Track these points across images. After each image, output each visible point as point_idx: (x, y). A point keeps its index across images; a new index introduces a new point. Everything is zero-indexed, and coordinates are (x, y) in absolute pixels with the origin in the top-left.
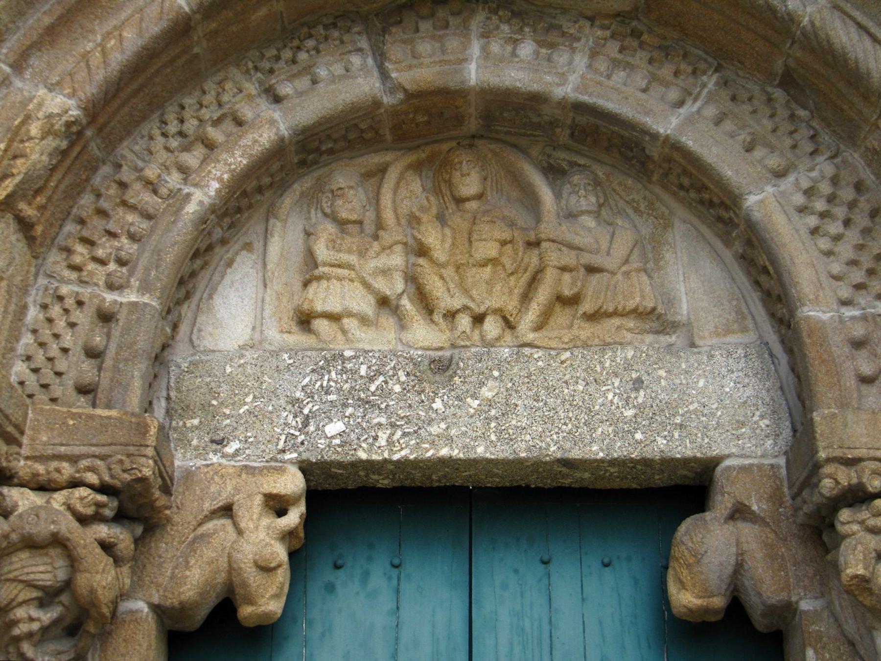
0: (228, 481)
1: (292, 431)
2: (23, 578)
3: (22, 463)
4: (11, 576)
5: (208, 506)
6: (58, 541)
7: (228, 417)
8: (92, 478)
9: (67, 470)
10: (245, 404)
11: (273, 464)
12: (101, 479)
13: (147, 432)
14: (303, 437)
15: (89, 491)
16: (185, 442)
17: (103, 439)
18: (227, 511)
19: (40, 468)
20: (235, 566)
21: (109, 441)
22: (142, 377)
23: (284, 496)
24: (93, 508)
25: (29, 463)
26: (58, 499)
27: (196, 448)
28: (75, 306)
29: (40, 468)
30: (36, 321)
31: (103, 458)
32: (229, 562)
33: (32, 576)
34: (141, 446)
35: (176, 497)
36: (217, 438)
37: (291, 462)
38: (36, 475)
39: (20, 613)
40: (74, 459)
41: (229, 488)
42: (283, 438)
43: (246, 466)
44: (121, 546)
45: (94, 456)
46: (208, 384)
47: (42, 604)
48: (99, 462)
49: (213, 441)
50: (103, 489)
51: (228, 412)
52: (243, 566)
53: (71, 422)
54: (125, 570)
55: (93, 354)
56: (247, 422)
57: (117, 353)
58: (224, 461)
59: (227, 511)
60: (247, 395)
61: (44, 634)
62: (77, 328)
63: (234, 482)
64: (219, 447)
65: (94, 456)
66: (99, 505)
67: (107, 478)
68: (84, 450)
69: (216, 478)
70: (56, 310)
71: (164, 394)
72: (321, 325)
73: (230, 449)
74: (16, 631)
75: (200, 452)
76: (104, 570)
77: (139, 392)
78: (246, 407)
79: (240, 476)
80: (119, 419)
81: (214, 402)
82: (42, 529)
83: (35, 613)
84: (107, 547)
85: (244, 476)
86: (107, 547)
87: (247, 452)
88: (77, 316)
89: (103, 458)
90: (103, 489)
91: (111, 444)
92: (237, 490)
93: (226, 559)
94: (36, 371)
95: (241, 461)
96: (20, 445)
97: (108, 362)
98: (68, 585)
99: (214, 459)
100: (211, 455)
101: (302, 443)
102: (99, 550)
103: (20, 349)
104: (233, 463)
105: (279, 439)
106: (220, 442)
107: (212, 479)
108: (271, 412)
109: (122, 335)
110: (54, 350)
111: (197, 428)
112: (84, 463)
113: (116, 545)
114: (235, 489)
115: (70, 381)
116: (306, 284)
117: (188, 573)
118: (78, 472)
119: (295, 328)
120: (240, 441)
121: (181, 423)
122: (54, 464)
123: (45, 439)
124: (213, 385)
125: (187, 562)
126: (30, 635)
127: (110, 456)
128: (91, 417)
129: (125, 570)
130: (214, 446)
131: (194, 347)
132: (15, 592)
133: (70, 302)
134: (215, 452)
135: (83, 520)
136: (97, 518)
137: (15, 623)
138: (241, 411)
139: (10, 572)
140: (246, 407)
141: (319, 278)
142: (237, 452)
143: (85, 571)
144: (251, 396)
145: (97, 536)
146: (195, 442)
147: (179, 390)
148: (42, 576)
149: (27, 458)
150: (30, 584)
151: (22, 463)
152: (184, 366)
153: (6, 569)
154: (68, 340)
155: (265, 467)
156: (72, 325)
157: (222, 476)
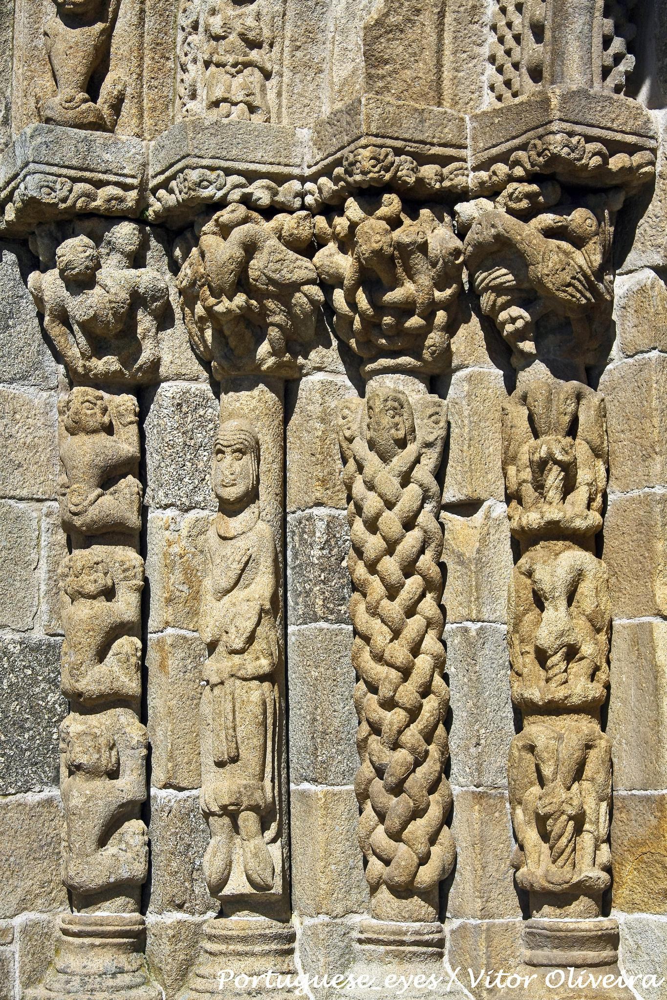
8: (519, 171)
12: (525, 169)
25: (476, 173)
30: (494, 15)
31: (524, 147)
33: (498, 281)
34: (546, 124)
40: (503, 158)
48: (520, 153)
50: (530, 178)
77: (576, 57)
84: (550, 233)
86: (550, 233)
89: (524, 147)
91: (525, 132)
96: (465, 161)
135: (525, 216)
149: (475, 169)
150: (499, 290)
151: (472, 174)
153: (479, 280)
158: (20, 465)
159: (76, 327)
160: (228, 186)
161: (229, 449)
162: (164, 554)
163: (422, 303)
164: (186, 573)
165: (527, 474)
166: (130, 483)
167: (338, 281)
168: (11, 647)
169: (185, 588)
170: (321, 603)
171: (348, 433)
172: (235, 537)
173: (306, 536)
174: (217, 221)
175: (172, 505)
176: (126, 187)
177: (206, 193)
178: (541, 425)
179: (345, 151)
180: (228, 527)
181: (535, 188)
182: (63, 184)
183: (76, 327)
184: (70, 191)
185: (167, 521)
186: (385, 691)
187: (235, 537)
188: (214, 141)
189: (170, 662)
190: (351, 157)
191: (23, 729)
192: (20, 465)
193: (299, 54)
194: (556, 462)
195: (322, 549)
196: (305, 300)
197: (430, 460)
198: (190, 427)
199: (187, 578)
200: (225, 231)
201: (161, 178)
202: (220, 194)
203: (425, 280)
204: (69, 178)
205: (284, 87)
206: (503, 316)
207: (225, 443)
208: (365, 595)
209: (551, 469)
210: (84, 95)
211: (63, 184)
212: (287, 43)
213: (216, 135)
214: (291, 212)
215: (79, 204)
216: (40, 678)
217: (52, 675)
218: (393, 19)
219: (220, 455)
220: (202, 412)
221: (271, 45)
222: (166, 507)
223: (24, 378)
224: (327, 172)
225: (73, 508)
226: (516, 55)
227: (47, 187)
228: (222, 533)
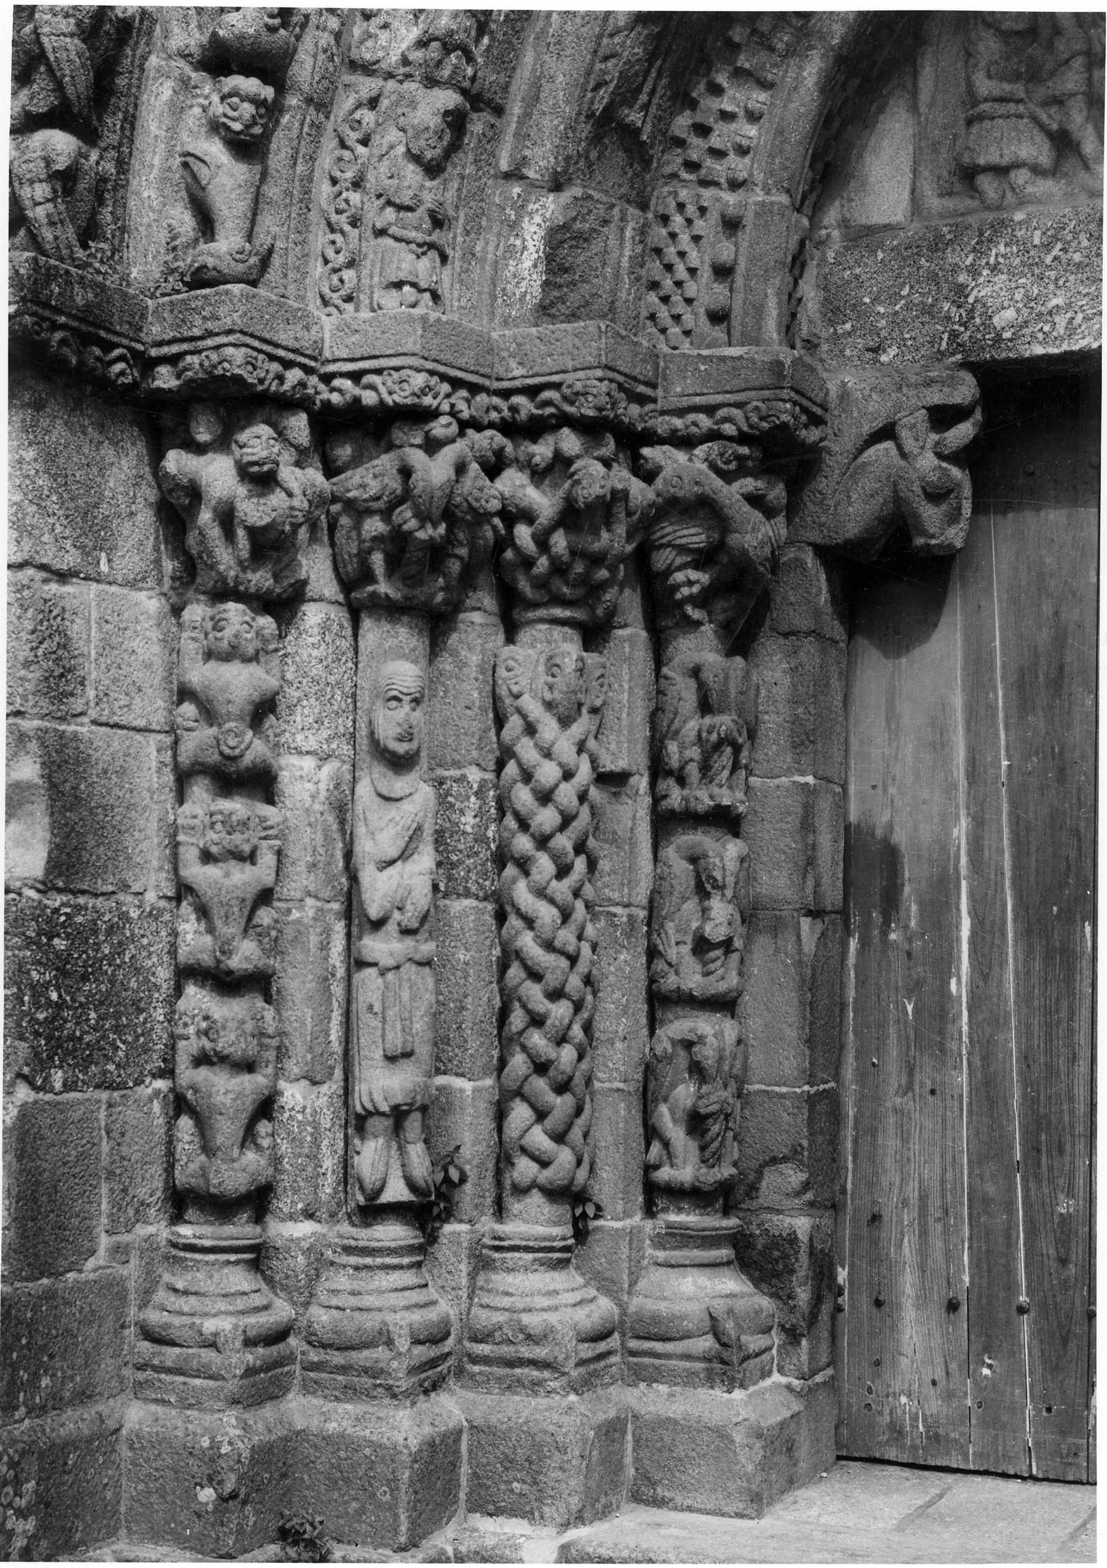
4: (664, 541)
5: (866, 429)
9: (705, 421)
12: (739, 430)
17: (737, 383)
18: (887, 432)
19: (678, 423)
21: (743, 386)
29: (678, 423)
31: (739, 405)
33: (683, 541)
38: (674, 431)
40: (710, 410)
42: (946, 336)
45: (729, 405)
47: (697, 565)
51: (882, 310)
53: (703, 368)
54: (781, 519)
55: (722, 272)
59: (887, 432)
61: (703, 600)
65: (729, 405)
67: (745, 428)
68: (720, 398)
69: (874, 396)
72: (987, 184)
74: (678, 596)
77: (775, 313)
82: (686, 491)
83: (693, 575)
86: (754, 500)
88: (700, 226)
89: (739, 405)
92: (898, 407)
97: (739, 281)
102: (746, 508)
105: (941, 339)
112: (721, 413)
116: (969, 123)
118: (716, 423)
119: (958, 187)
122: (692, 417)
123: (679, 389)
125: (849, 497)
126: (691, 599)
127: (746, 403)
128: (723, 359)
129: (781, 519)
137: (676, 587)
139: (663, 537)
141: (981, 118)
143: (736, 531)
144: (907, 288)
145: (744, 490)
150: (682, 549)
159: (241, 533)
161: (408, 698)
165: (695, 753)
167: (528, 516)
171: (515, 689)
172: (401, 799)
179: (569, 378)
181: (745, 450)
183: (241, 533)
186: (552, 980)
187: (401, 799)
190: (578, 386)
200: (432, 446)
203: (621, 530)
206: (679, 577)
207: (405, 691)
208: (527, 874)
218: (578, 225)
224: (532, 392)
225: (227, 751)
228: (385, 792)
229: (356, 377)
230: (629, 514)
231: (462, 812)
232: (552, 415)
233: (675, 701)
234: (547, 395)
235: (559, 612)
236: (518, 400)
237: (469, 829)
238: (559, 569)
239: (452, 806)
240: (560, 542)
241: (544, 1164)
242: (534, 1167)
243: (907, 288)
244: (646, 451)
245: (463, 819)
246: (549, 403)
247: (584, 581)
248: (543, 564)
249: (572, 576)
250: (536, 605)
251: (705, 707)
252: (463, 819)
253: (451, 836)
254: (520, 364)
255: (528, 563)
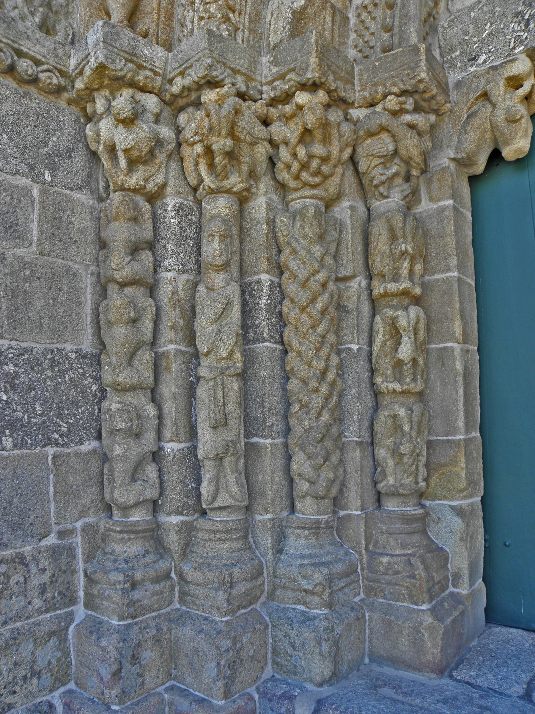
0: (482, 79)
1: (518, 34)
2: (371, 153)
3: (357, 94)
6: (383, 129)
7: (475, 43)
10: (486, 30)
11: (509, 59)
13: (419, 51)
14: (526, 34)
15: (393, 96)
16: (452, 65)
20: (495, 125)
22: (416, 31)
23: (518, 75)
24: (398, 105)
25: (361, 93)
26: (379, 108)
27: (460, 68)
28: (373, 8)
30: (355, 25)
32: (491, 125)
35: (453, 98)
36: (471, 57)
37: (520, 53)
39: (374, 173)
41: (483, 82)
43: (491, 67)
44: (420, 125)
46: (461, 29)
49: (469, 60)
51: (475, 40)
52: (499, 124)
53: (377, 64)
54: (427, 137)
56: (488, 40)
57: (400, 22)
58: (478, 69)
60: (486, 25)
62: (377, 19)
63: (485, 78)
64: (474, 62)
66: (401, 103)
67: (402, 86)
69: (474, 79)
70: (364, 15)
71: (437, 46)
73: (480, 61)
75: (463, 69)
76: (411, 137)
78: (487, 32)
79: (488, 73)
80: (403, 51)
81: (467, 38)
82: (373, 124)
84: (411, 126)
85: (491, 72)
87: (491, 58)
88: (377, 13)
90: (404, 93)
93: (489, 124)
94: (360, 51)
95: (488, 64)
97: (396, 30)
98: (396, 152)
99: (472, 69)
100: (470, 69)
101: (526, 38)
103: (350, 43)
104: (483, 68)
105: (510, 42)
106: (475, 59)
107: (472, 80)
108: (503, 28)
109: (401, 11)
110: (367, 37)
111: (458, 56)
113: (417, 124)
114: (487, 81)
115: (378, 49)
117: (467, 136)
120: (486, 54)
121: (449, 57)
124: (464, 28)
125: (466, 131)
130: (471, 63)
131: (450, 12)
132: (369, 162)
133: (370, 8)
134: (472, 66)
136: (402, 111)
137: (373, 178)
138: (484, 36)
140: (487, 32)
142: (485, 61)
144: (489, 24)
146: (459, 65)
147: (446, 40)
148: (380, 150)
149: (359, 91)
152: (446, 25)
154: (373, 29)
155: (503, 63)
156: (374, 19)
157: (478, 77)
158: (76, 242)
160: (226, 74)
161: (218, 234)
162: (169, 299)
163: (335, 158)
164: (182, 312)
166: (146, 257)
168: (70, 354)
169: (181, 321)
170: (267, 331)
173: (255, 293)
174: (218, 93)
175: (175, 269)
176: (155, 73)
177: (215, 73)
178: (399, 232)
180: (214, 283)
182: (120, 60)
184: (125, 65)
185: (171, 279)
188: (219, 45)
189: (174, 366)
191: (78, 406)
192: (76, 242)
193: (252, 25)
194: (409, 254)
195: (267, 300)
196: (264, 150)
197: (332, 250)
198: (184, 224)
199: (182, 315)
201: (179, 70)
202: (221, 77)
204: (124, 58)
205: (245, 39)
209: (405, 259)
210: (126, 22)
211: (120, 60)
212: (247, 16)
213: (220, 42)
214: (255, 101)
215: (129, 75)
216: (87, 375)
217: (94, 373)
219: (210, 238)
220: (190, 217)
221: (240, 14)
222: (170, 270)
223: (80, 189)
224: (282, 77)
226: (372, 44)
227: (111, 58)
229: (182, 74)
230: (340, 136)
231: (260, 298)
232: (293, 86)
233: (377, 236)
234: (288, 77)
235: (308, 192)
236: (277, 83)
237: (263, 306)
238: (304, 167)
239: (255, 296)
240: (302, 152)
241: (313, 483)
242: (307, 484)
243: (489, 24)
244: (351, 111)
245: (260, 302)
246: (289, 80)
247: (318, 172)
248: (295, 166)
249: (312, 170)
250: (296, 190)
251: (393, 238)
252: (260, 302)
253: (255, 311)
254: (276, 66)
255: (288, 167)
